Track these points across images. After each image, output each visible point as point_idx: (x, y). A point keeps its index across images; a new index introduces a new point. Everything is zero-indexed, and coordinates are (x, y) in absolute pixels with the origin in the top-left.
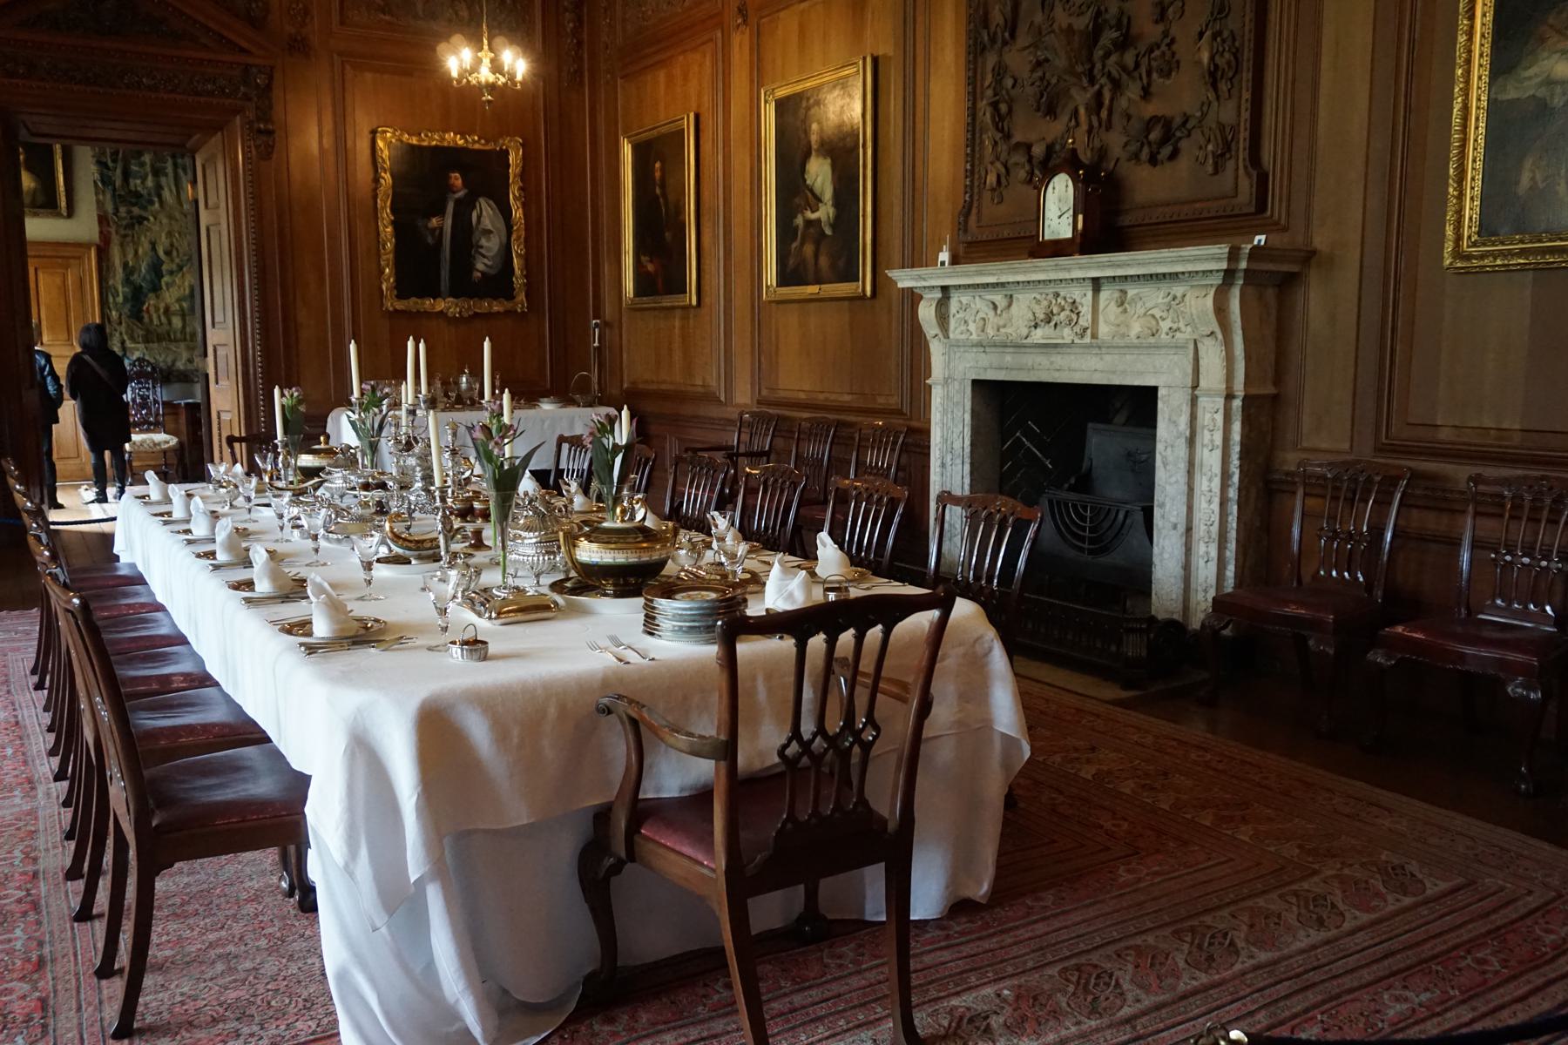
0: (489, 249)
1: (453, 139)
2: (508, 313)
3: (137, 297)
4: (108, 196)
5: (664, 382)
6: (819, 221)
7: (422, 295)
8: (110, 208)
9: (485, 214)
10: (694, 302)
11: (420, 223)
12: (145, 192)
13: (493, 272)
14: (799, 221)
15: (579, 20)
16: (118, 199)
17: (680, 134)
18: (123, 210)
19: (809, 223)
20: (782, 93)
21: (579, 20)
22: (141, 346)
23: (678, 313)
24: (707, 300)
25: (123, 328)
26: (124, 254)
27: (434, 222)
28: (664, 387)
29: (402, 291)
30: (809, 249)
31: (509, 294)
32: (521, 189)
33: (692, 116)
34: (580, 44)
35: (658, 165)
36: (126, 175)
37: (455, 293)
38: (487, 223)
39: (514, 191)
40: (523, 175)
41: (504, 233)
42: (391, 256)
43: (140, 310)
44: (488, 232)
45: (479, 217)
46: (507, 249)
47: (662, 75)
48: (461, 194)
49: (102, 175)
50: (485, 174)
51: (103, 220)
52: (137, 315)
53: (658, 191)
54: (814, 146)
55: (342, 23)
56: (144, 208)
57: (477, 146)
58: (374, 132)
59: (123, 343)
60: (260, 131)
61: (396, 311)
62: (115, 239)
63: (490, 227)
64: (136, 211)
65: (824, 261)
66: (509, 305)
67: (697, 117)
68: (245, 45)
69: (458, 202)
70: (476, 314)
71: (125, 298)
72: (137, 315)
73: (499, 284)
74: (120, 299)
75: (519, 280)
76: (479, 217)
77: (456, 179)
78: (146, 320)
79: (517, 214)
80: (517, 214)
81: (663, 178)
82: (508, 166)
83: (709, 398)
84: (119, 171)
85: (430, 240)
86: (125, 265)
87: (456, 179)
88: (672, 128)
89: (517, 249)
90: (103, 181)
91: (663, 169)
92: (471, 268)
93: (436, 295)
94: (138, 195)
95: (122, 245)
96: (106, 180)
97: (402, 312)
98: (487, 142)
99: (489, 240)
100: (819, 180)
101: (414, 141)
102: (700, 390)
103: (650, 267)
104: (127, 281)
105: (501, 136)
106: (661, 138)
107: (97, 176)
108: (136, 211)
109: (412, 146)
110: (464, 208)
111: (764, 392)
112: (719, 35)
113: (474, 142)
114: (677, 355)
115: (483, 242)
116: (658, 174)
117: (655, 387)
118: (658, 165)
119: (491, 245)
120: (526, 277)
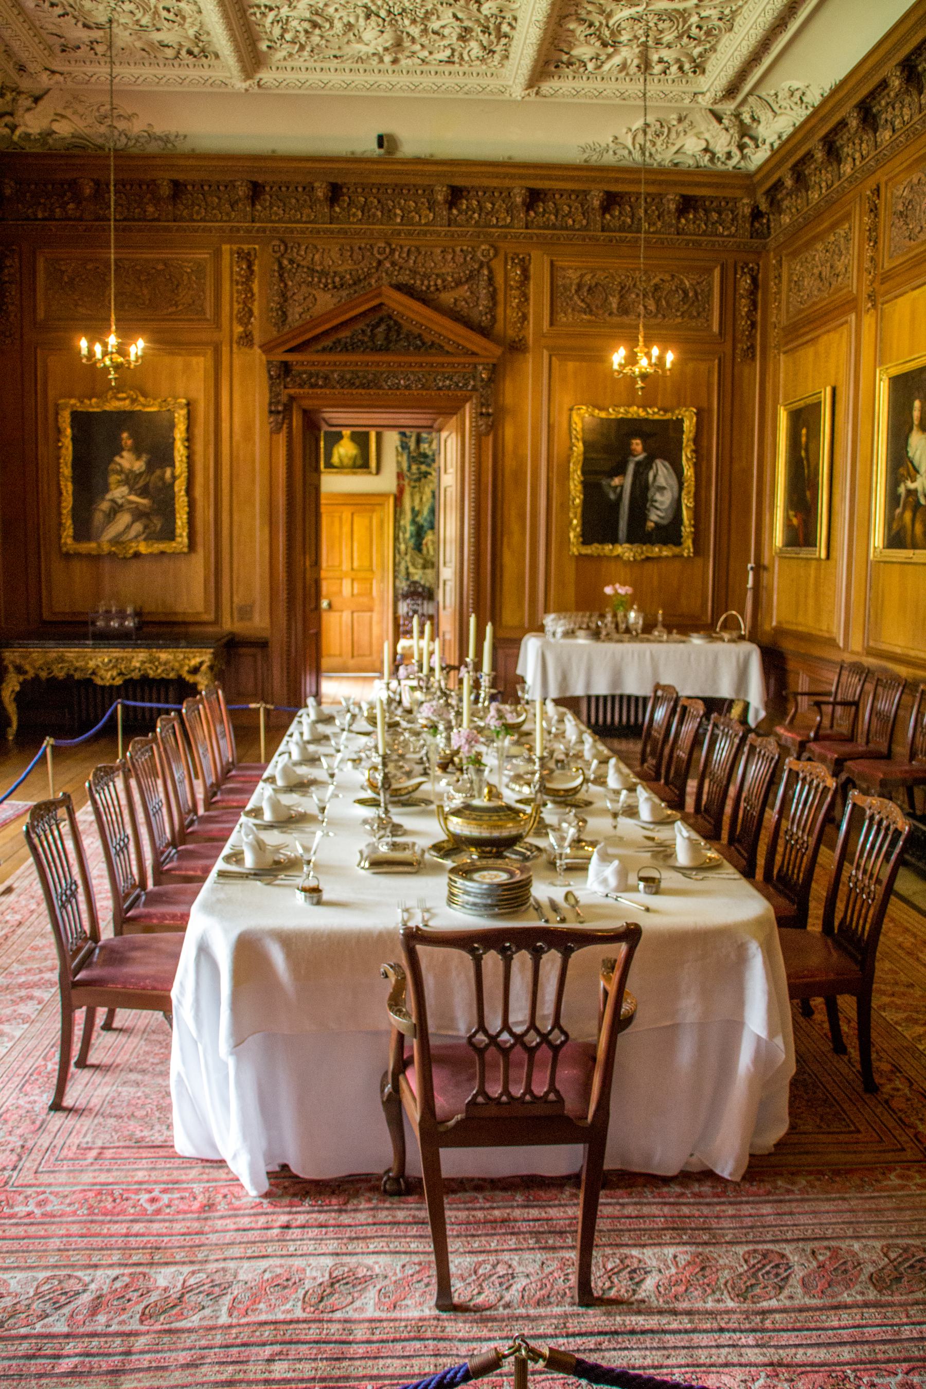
0: (662, 503)
1: (636, 412)
2: (675, 556)
3: (419, 534)
4: (405, 457)
5: (800, 624)
6: (916, 491)
7: (602, 542)
8: (405, 466)
9: (661, 473)
10: (823, 555)
11: (604, 482)
12: (430, 453)
13: (665, 522)
14: (902, 490)
15: (754, 303)
16: (412, 459)
17: (818, 405)
18: (414, 467)
19: (910, 492)
20: (895, 371)
21: (754, 303)
22: (420, 572)
23: (814, 563)
24: (834, 554)
25: (408, 558)
26: (413, 500)
27: (616, 481)
28: (800, 628)
29: (587, 538)
30: (908, 516)
31: (678, 542)
32: (693, 451)
33: (829, 389)
34: (753, 325)
35: (804, 431)
36: (419, 441)
37: (630, 540)
38: (661, 481)
39: (687, 454)
40: (696, 440)
41: (676, 488)
42: (579, 510)
43: (421, 544)
44: (661, 489)
45: (655, 477)
46: (678, 502)
47: (810, 351)
48: (640, 457)
49: (402, 442)
50: (662, 440)
51: (400, 476)
52: (418, 547)
53: (803, 454)
54: (916, 422)
55: (552, 324)
56: (429, 465)
57: (656, 417)
58: (571, 410)
59: (407, 568)
60: (482, 414)
61: (580, 555)
62: (408, 490)
63: (664, 484)
64: (423, 468)
65: (919, 528)
66: (677, 550)
67: (834, 390)
68: (475, 349)
69: (638, 464)
70: (648, 558)
71: (412, 536)
72: (418, 547)
73: (669, 534)
74: (408, 535)
75: (687, 529)
76: (655, 477)
77: (637, 445)
78: (425, 551)
79: (688, 472)
80: (688, 472)
81: (807, 443)
82: (682, 432)
83: (831, 642)
84: (413, 439)
85: (612, 496)
86: (413, 509)
87: (637, 445)
88: (812, 400)
89: (687, 502)
90: (403, 448)
91: (808, 435)
92: (645, 518)
93: (614, 540)
94: (425, 456)
95: (412, 495)
96: (404, 446)
97: (586, 555)
98: (666, 411)
99: (662, 495)
100: (918, 452)
101: (603, 415)
102: (827, 635)
103: (795, 521)
104: (414, 522)
105: (678, 406)
106: (807, 407)
107: (398, 443)
108: (423, 468)
109: (602, 419)
110: (643, 468)
111: (872, 644)
112: (853, 316)
113: (654, 413)
114: (811, 602)
115: (658, 497)
116: (804, 439)
117: (794, 627)
118: (804, 431)
119: (663, 500)
120: (694, 526)
